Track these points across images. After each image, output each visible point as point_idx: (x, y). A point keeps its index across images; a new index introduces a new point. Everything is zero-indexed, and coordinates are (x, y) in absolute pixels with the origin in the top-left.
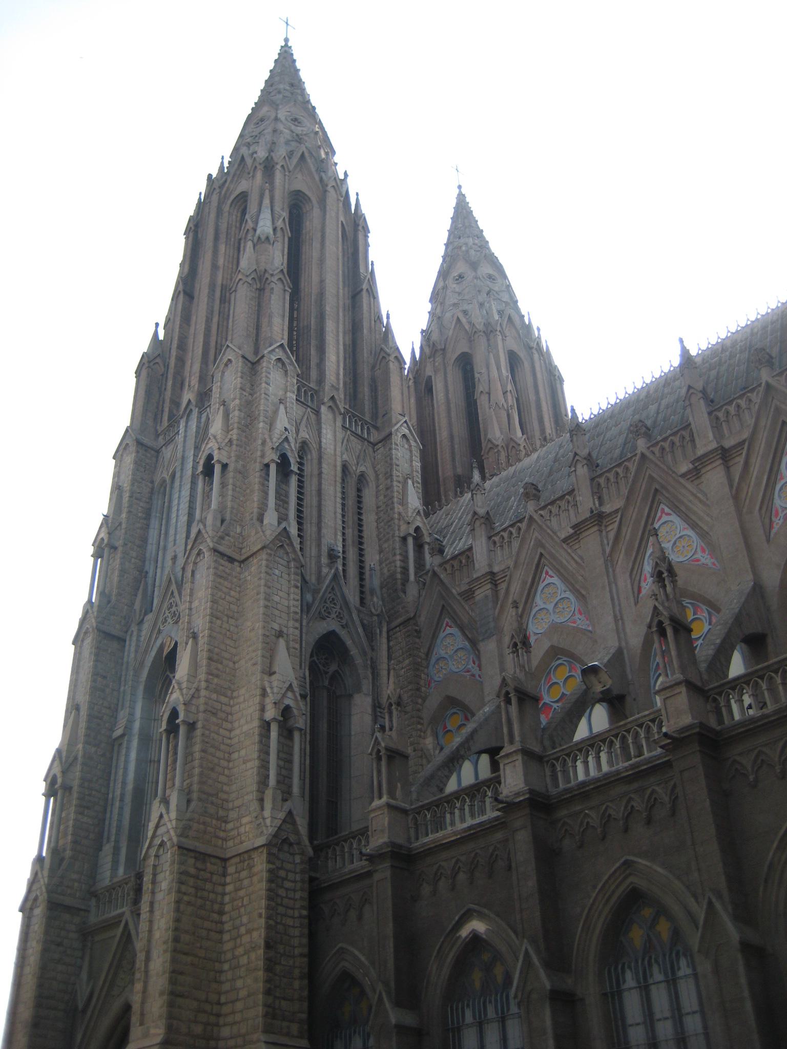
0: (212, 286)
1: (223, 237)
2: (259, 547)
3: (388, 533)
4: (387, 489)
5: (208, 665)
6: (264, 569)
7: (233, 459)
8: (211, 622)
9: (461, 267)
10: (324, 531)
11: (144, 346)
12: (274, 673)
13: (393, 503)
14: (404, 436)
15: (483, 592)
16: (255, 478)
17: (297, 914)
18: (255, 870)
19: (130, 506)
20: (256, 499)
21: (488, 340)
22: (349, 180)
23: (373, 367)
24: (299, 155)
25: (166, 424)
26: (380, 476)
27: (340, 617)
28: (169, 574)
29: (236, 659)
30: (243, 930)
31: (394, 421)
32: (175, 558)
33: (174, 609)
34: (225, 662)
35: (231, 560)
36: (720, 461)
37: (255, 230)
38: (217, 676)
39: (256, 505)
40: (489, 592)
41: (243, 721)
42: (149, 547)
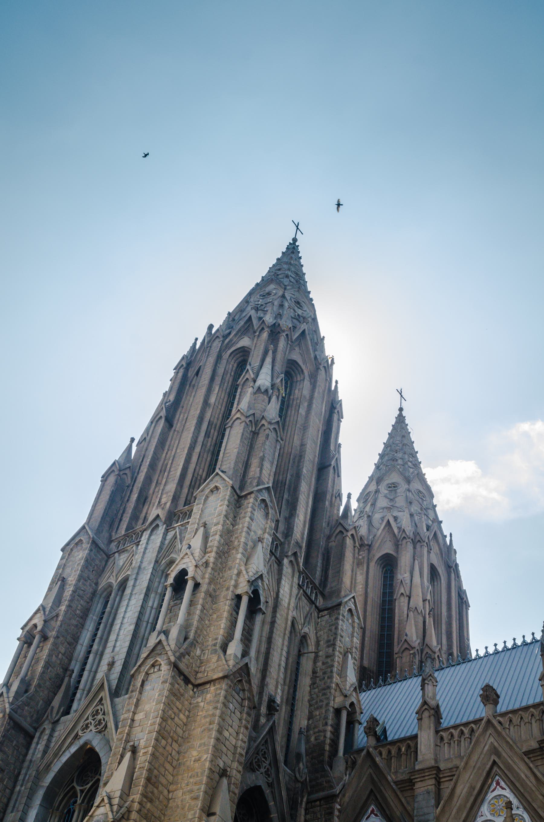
0: (201, 419)
1: (218, 380)
2: (221, 675)
3: (321, 701)
4: (327, 657)
5: (145, 787)
6: (222, 698)
7: (207, 580)
8: (157, 740)
9: (395, 478)
10: (268, 680)
11: (116, 454)
12: (214, 814)
13: (332, 672)
14: (350, 610)
16: (225, 607)
19: (71, 601)
20: (223, 626)
21: (415, 548)
22: (334, 366)
23: (329, 537)
24: (301, 331)
25: (123, 533)
26: (322, 643)
27: (267, 774)
28: (103, 679)
29: (171, 788)
31: (343, 593)
32: (111, 665)
33: (100, 717)
34: (161, 788)
35: (187, 681)
37: (255, 381)
38: (151, 801)
39: (221, 632)
40: (432, 788)
42: (79, 647)
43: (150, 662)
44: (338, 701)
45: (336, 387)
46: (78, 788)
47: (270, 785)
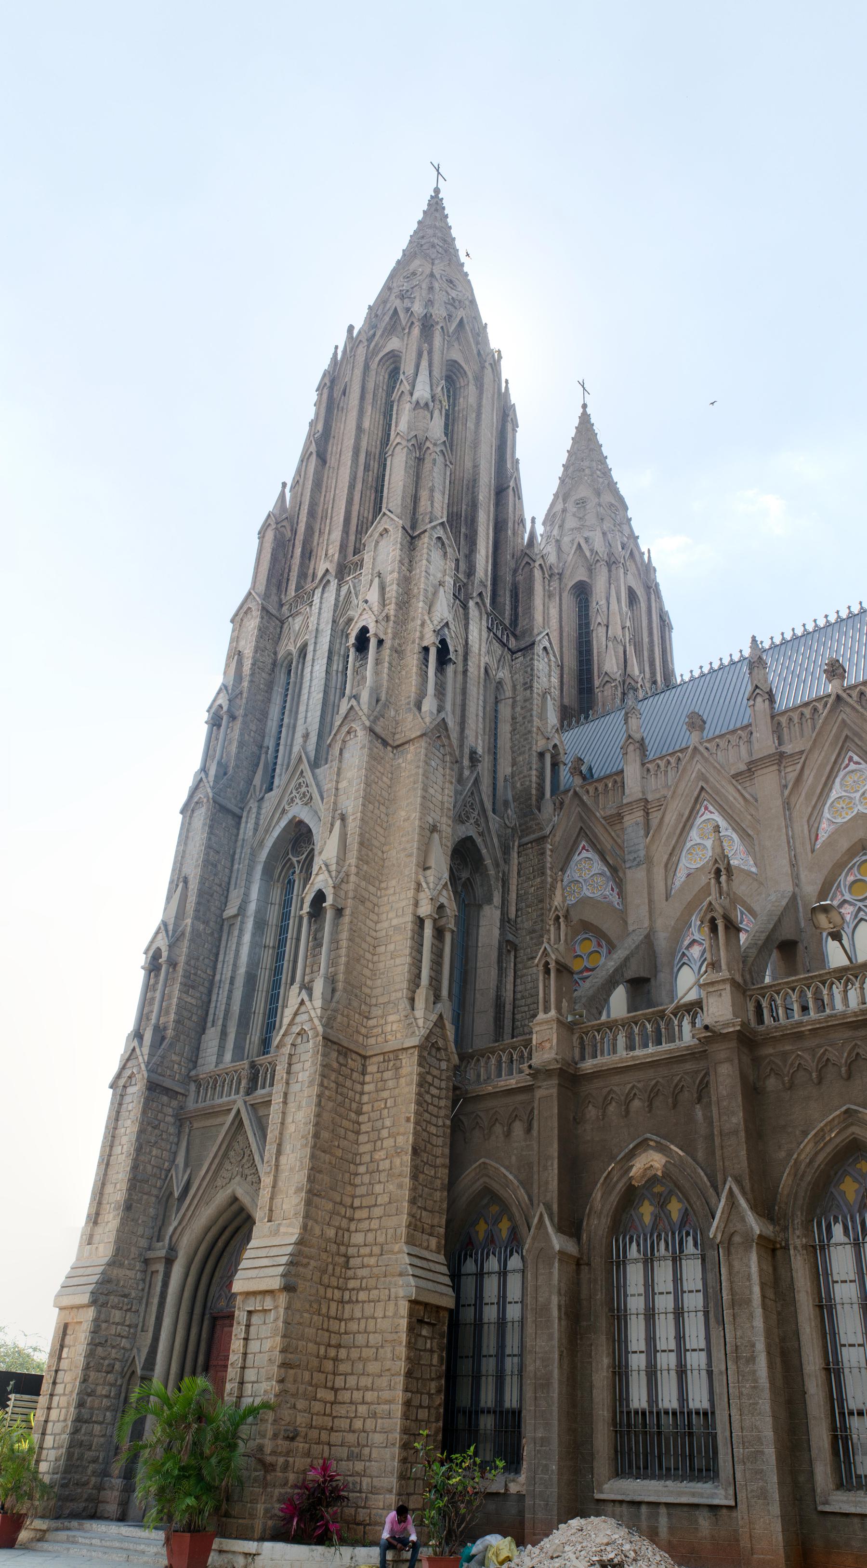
2: (419, 733)
3: (524, 746)
4: (525, 701)
5: (359, 851)
6: (422, 757)
8: (363, 805)
10: (467, 732)
11: (268, 504)
12: (429, 868)
13: (531, 716)
14: (545, 648)
15: (633, 820)
17: (440, 1123)
18: (404, 1071)
19: (252, 674)
22: (503, 362)
23: (515, 571)
25: (293, 594)
26: (518, 687)
27: (477, 823)
28: (300, 752)
29: (385, 848)
30: (385, 1133)
31: (536, 631)
32: (306, 736)
33: (303, 789)
34: (375, 850)
35: (385, 743)
38: (367, 863)
39: (413, 689)
40: (641, 820)
41: (392, 915)
42: (269, 723)
43: (345, 729)
44: (540, 744)
45: (507, 388)
46: (294, 860)
47: (481, 834)
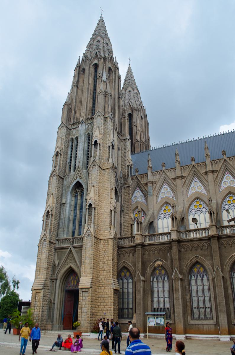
0: (88, 89)
13: (126, 157)
17: (116, 253)
18: (109, 243)
20: (107, 154)
33: (80, 175)
35: (102, 169)
36: (212, 173)
38: (99, 197)
41: (105, 208)
43: (93, 165)
44: (128, 164)
46: (78, 191)
47: (117, 186)
